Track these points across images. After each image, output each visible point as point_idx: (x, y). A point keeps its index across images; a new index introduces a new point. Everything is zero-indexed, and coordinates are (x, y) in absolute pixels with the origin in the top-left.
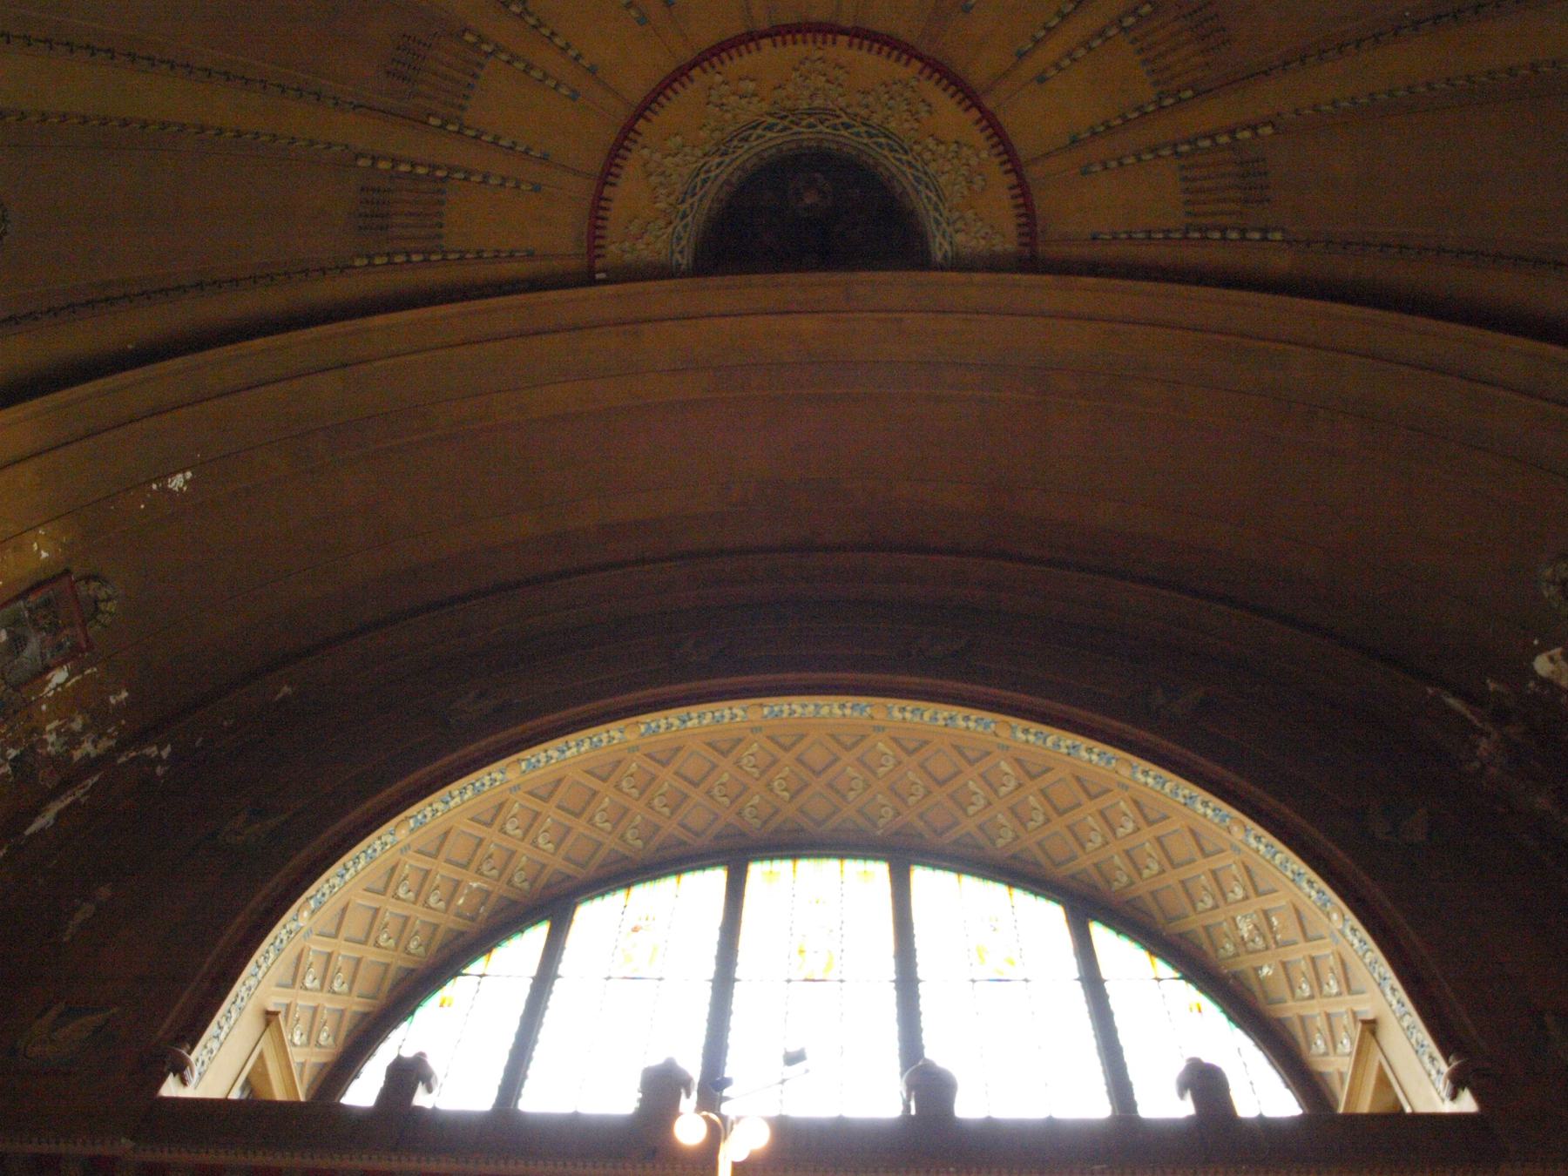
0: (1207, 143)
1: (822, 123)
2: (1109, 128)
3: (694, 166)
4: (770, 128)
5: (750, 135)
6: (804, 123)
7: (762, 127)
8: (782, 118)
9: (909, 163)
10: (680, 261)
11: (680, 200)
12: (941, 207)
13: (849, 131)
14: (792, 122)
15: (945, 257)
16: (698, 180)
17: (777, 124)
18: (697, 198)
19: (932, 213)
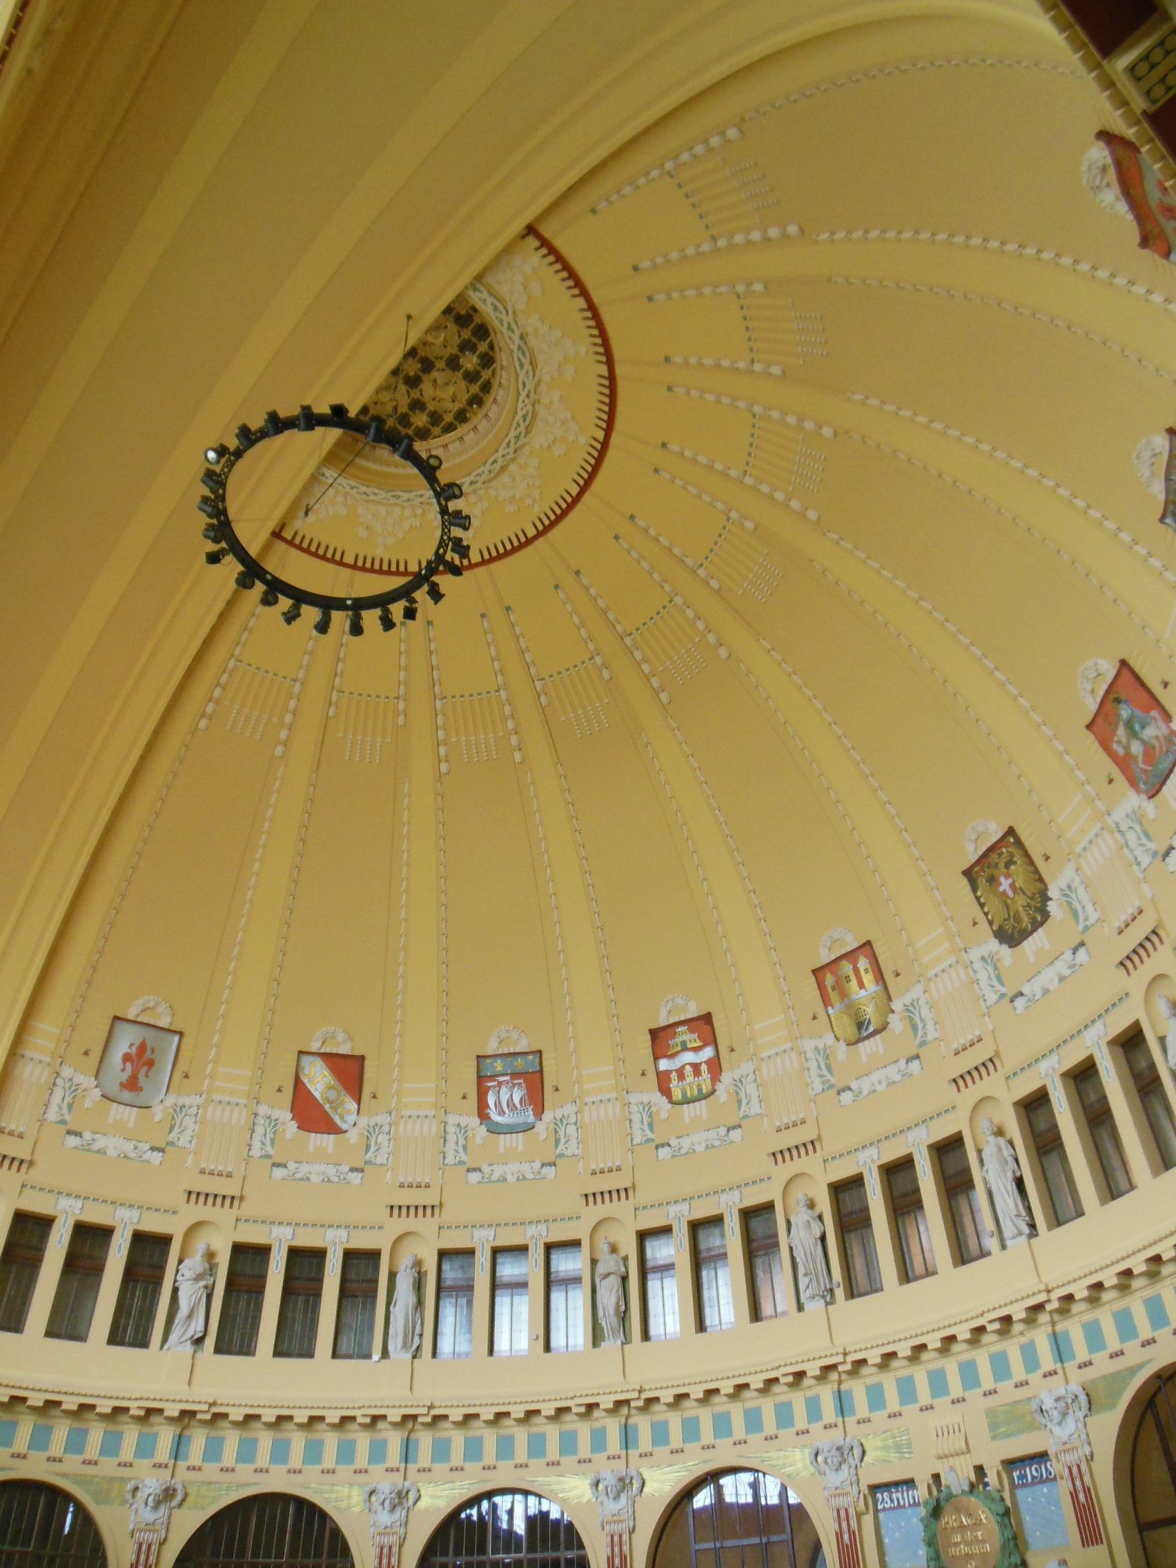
0: (292, 704)
1: (490, 471)
2: (342, 645)
3: (539, 367)
4: (517, 438)
5: (524, 421)
6: (500, 461)
7: (523, 435)
8: (516, 451)
9: (413, 500)
10: (477, 294)
11: (525, 336)
12: (364, 497)
13: (469, 482)
14: (508, 453)
15: (323, 475)
16: (526, 362)
17: (516, 443)
18: (515, 348)
19: (364, 489)
